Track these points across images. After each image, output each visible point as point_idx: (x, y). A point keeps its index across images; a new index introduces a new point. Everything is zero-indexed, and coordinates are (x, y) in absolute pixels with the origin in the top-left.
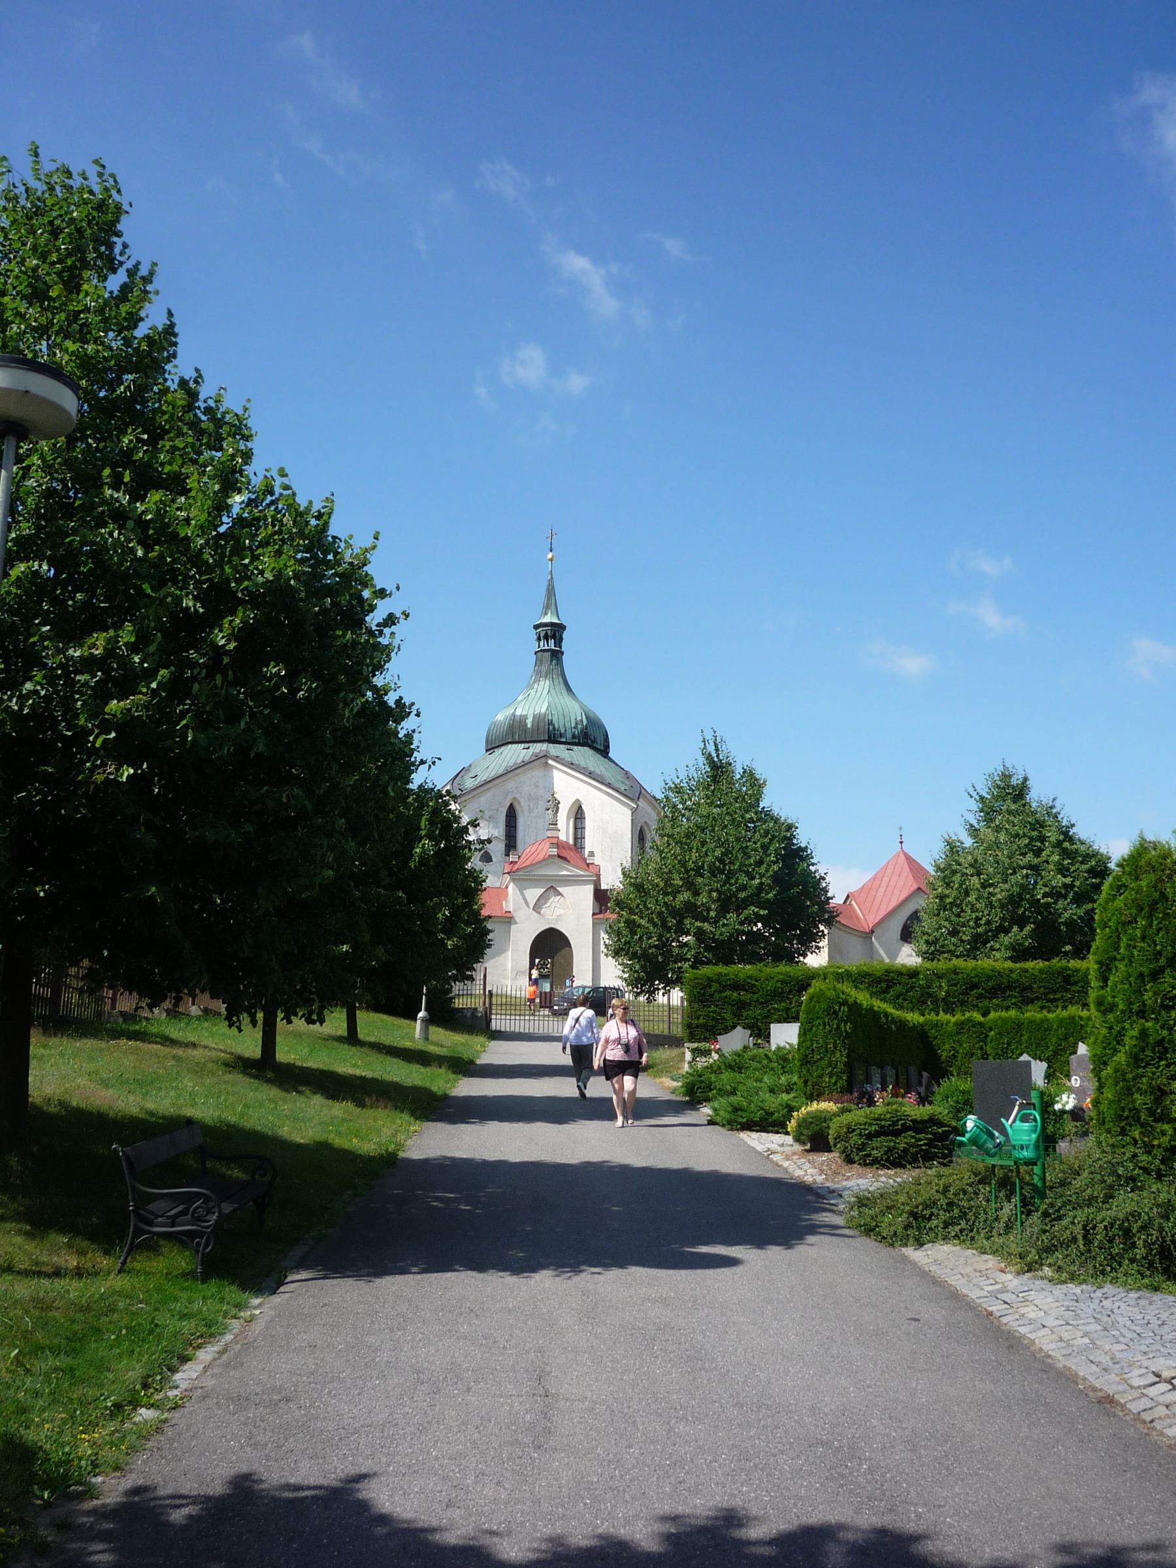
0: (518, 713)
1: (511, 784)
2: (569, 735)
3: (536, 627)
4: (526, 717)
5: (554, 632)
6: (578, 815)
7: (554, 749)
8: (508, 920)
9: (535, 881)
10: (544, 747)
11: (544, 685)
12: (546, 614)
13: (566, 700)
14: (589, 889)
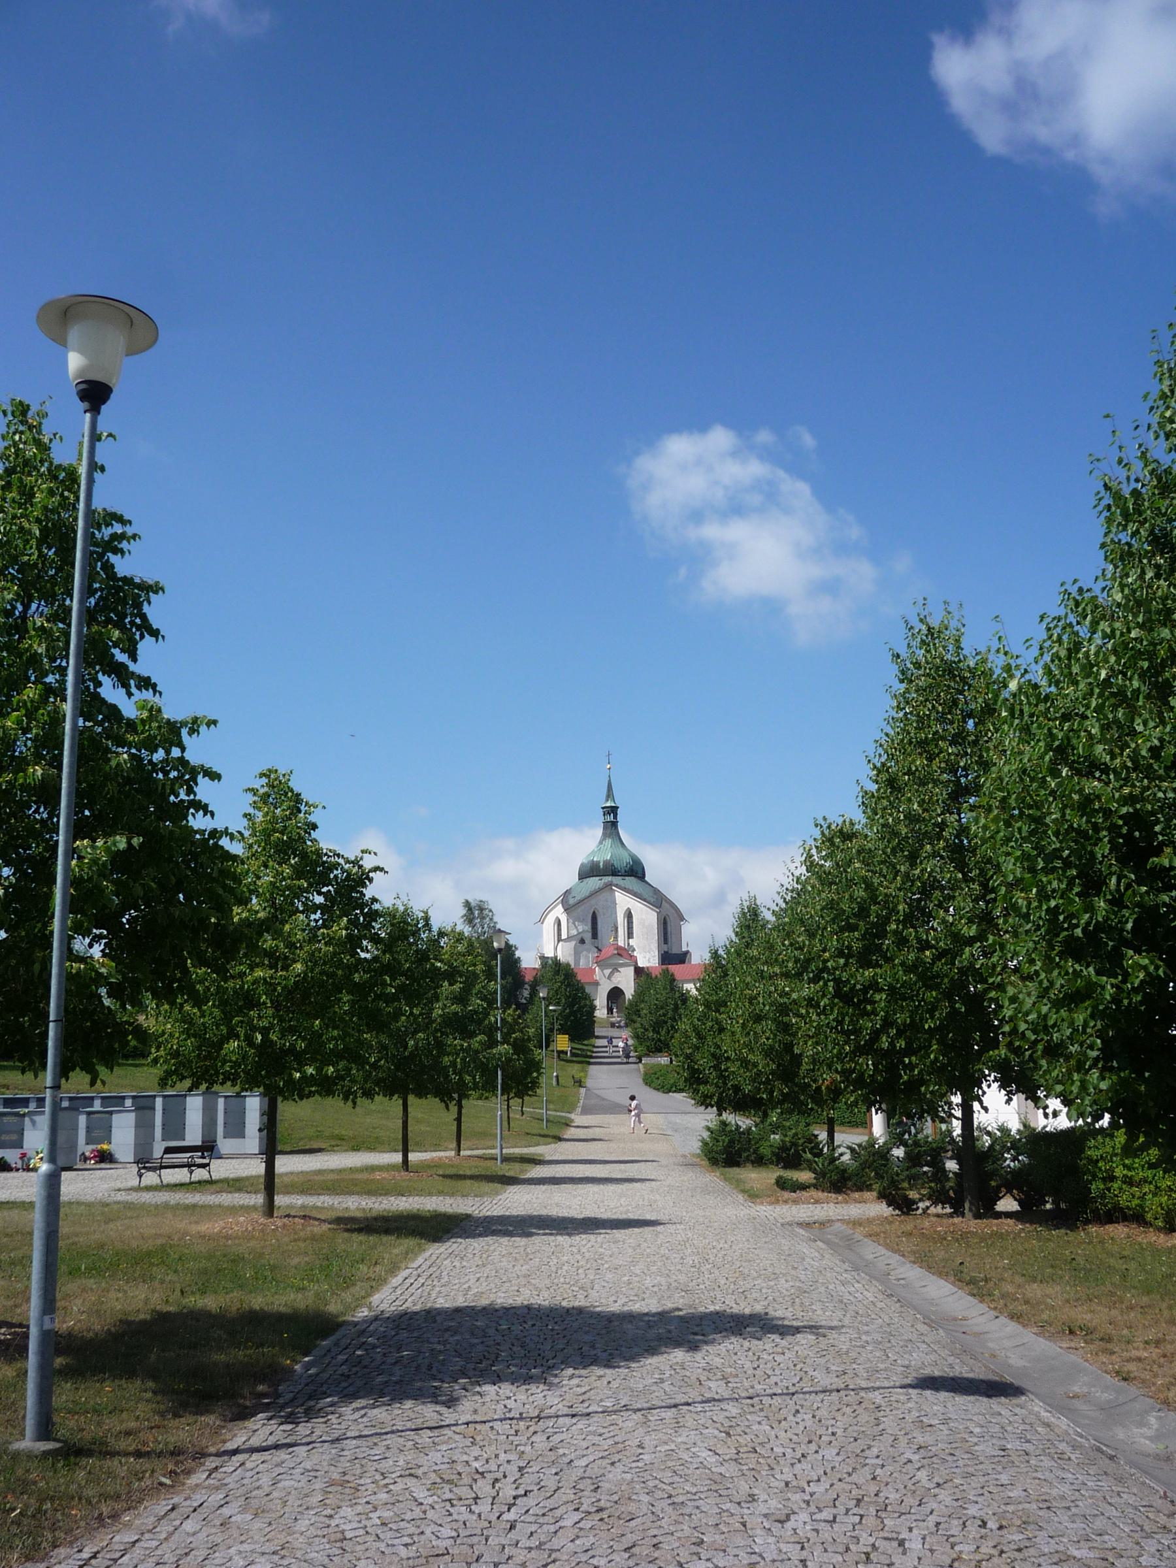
0: (595, 859)
1: (593, 901)
2: (623, 871)
3: (603, 808)
4: (599, 862)
5: (613, 810)
6: (629, 915)
7: (617, 880)
8: (597, 984)
9: (607, 966)
10: (609, 878)
11: (608, 842)
12: (607, 800)
13: (621, 850)
14: (632, 968)
